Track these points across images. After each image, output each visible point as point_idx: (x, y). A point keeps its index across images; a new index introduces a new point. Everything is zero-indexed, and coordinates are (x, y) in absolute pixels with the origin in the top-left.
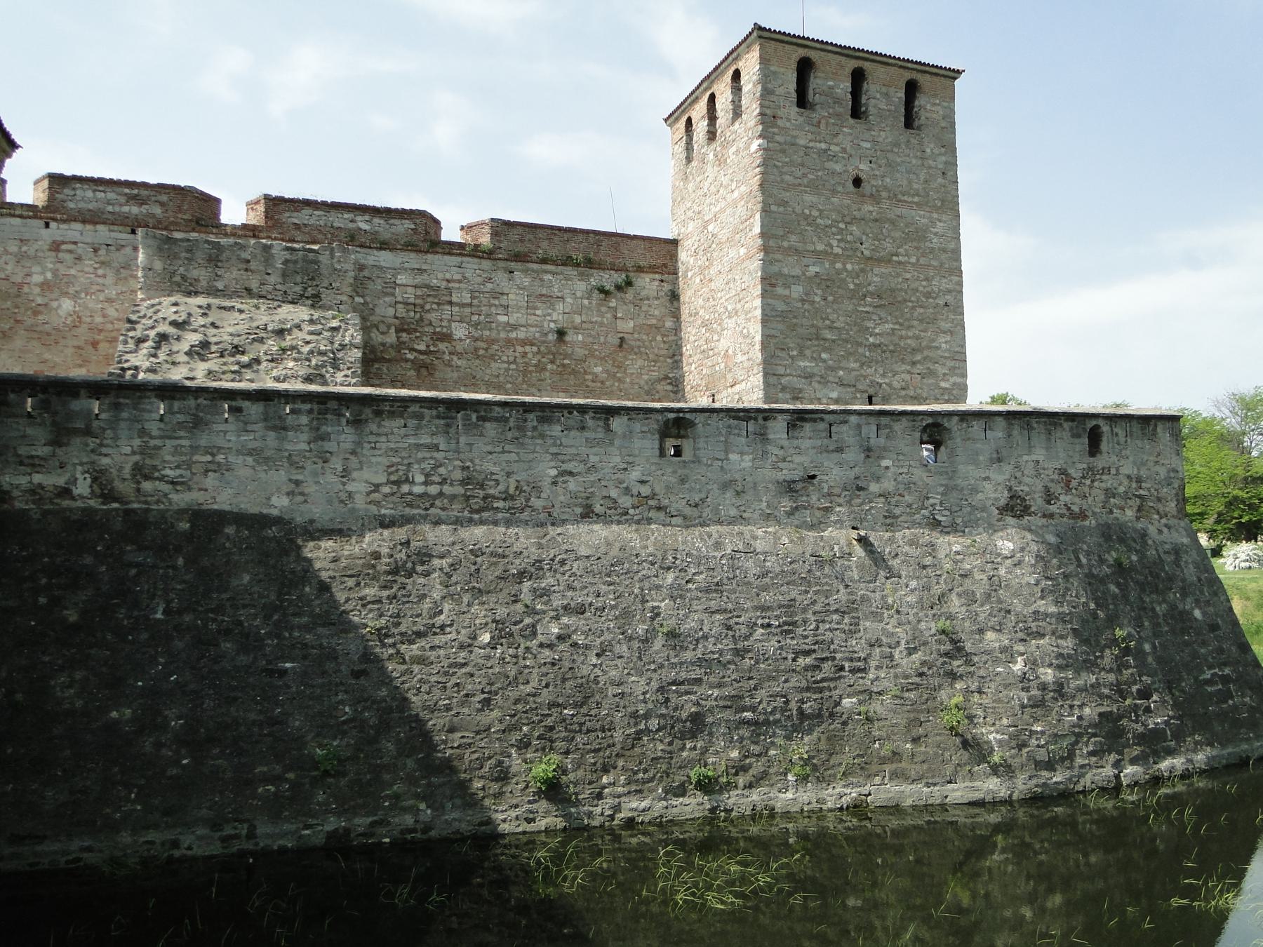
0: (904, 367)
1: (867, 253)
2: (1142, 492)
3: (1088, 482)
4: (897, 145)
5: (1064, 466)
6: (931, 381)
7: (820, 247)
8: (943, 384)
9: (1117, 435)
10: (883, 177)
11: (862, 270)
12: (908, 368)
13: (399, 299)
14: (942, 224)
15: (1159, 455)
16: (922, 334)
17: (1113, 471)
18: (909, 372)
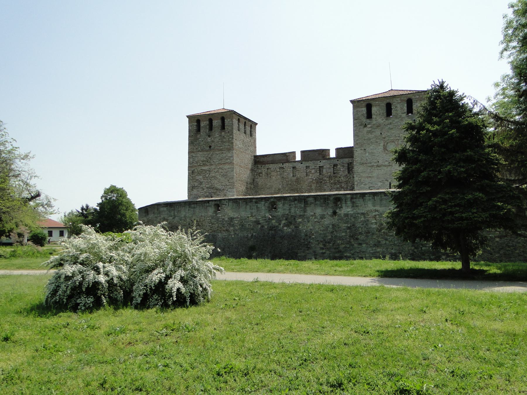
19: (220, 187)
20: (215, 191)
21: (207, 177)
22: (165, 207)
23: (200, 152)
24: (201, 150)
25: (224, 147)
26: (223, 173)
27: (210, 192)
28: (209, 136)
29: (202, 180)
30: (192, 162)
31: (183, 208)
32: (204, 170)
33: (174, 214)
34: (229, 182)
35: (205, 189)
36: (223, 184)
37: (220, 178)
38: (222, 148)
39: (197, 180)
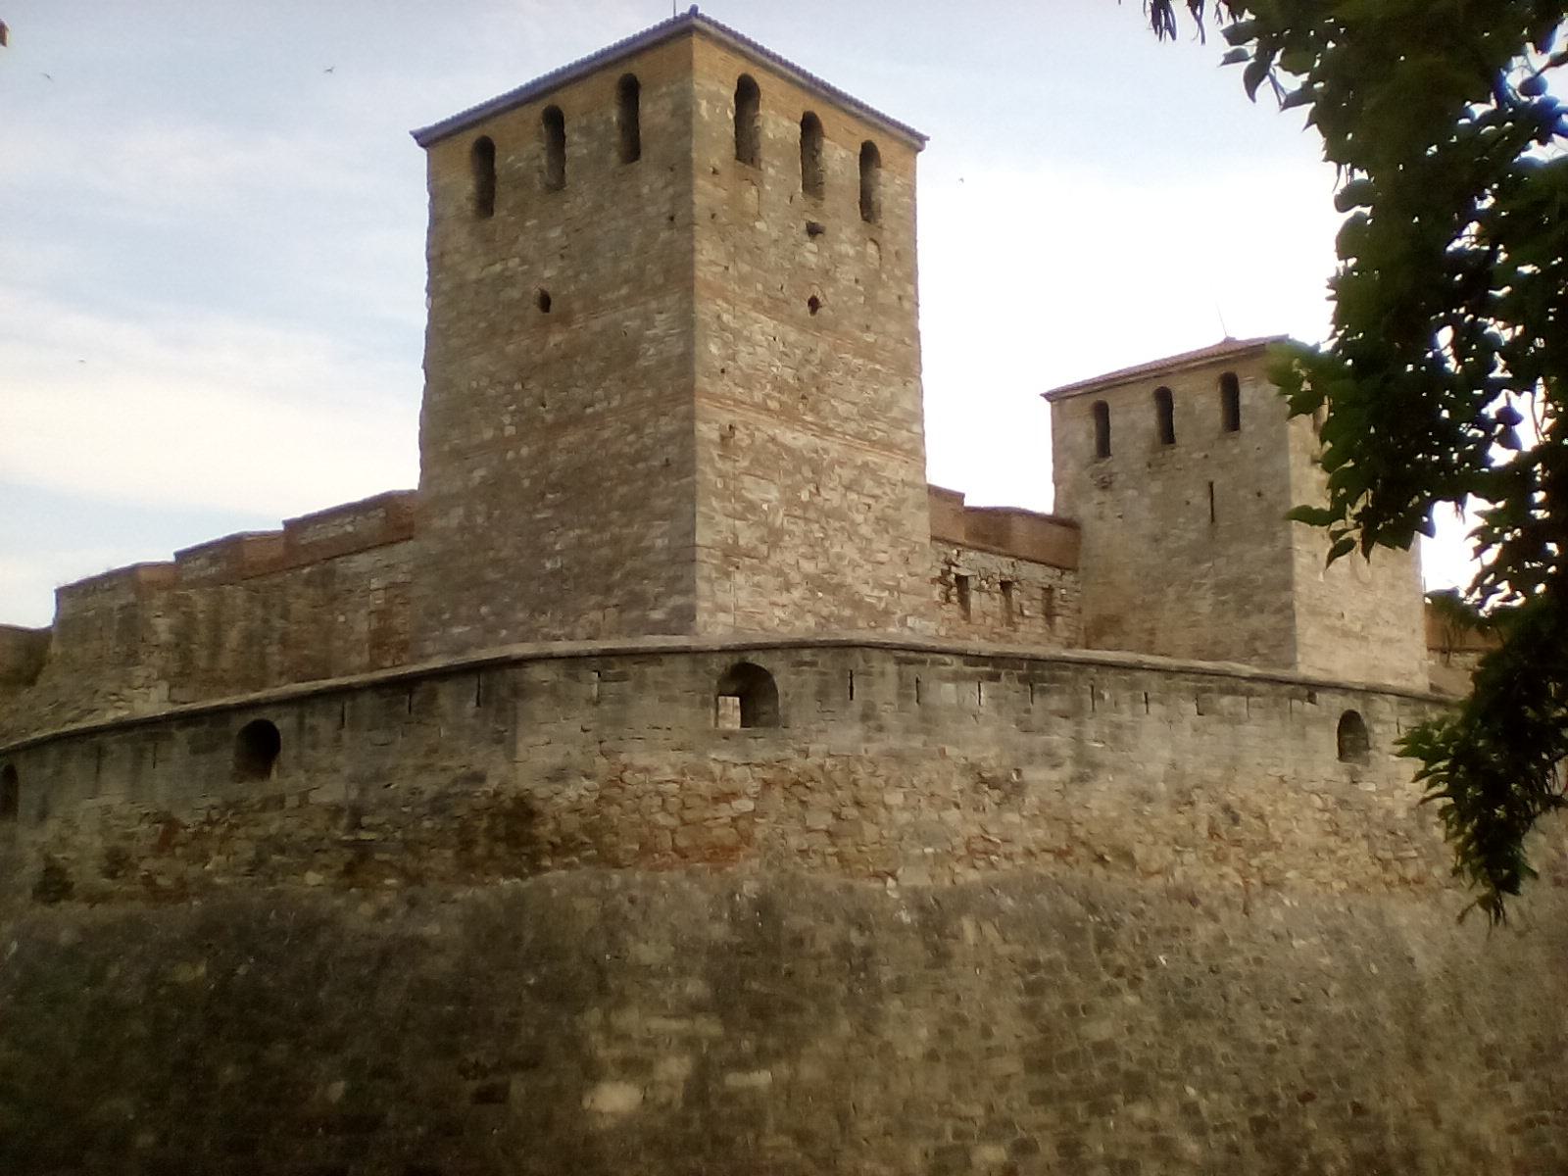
0: (595, 599)
1: (549, 418)
2: (364, 836)
3: (219, 831)
4: (599, 208)
5: (165, 808)
6: (635, 614)
7: (488, 434)
8: (657, 615)
9: (313, 729)
10: (577, 275)
11: (543, 453)
12: (599, 598)
13: (372, 608)
14: (663, 316)
15: (433, 750)
16: (625, 531)
17: (292, 802)
18: (602, 607)
19: (869, 594)
20: (847, 612)
21: (805, 506)
22: (979, 678)
23: (765, 311)
24: (766, 303)
25: (881, 340)
26: (881, 506)
27: (825, 612)
28: (813, 231)
29: (779, 519)
30: (718, 364)
31: (1154, 708)
32: (789, 450)
33: (1078, 740)
34: (910, 574)
35: (795, 585)
36: (884, 572)
37: (865, 530)
38: (870, 338)
39: (752, 507)
